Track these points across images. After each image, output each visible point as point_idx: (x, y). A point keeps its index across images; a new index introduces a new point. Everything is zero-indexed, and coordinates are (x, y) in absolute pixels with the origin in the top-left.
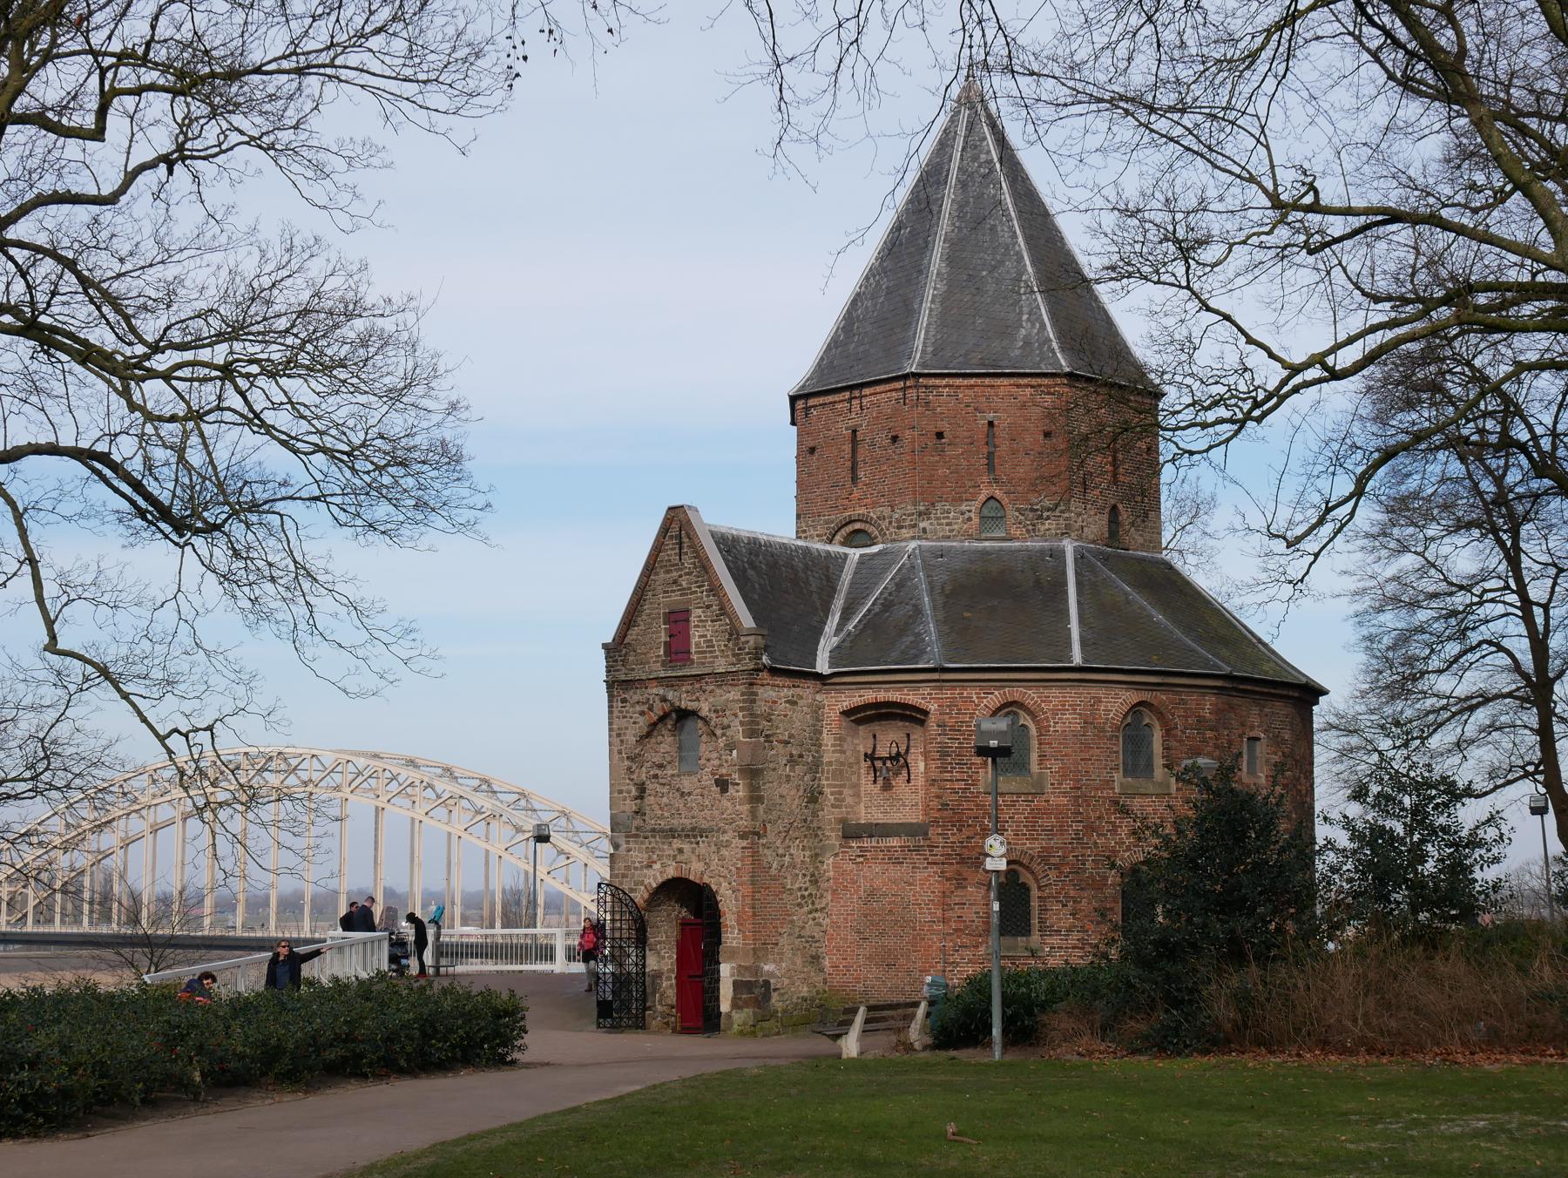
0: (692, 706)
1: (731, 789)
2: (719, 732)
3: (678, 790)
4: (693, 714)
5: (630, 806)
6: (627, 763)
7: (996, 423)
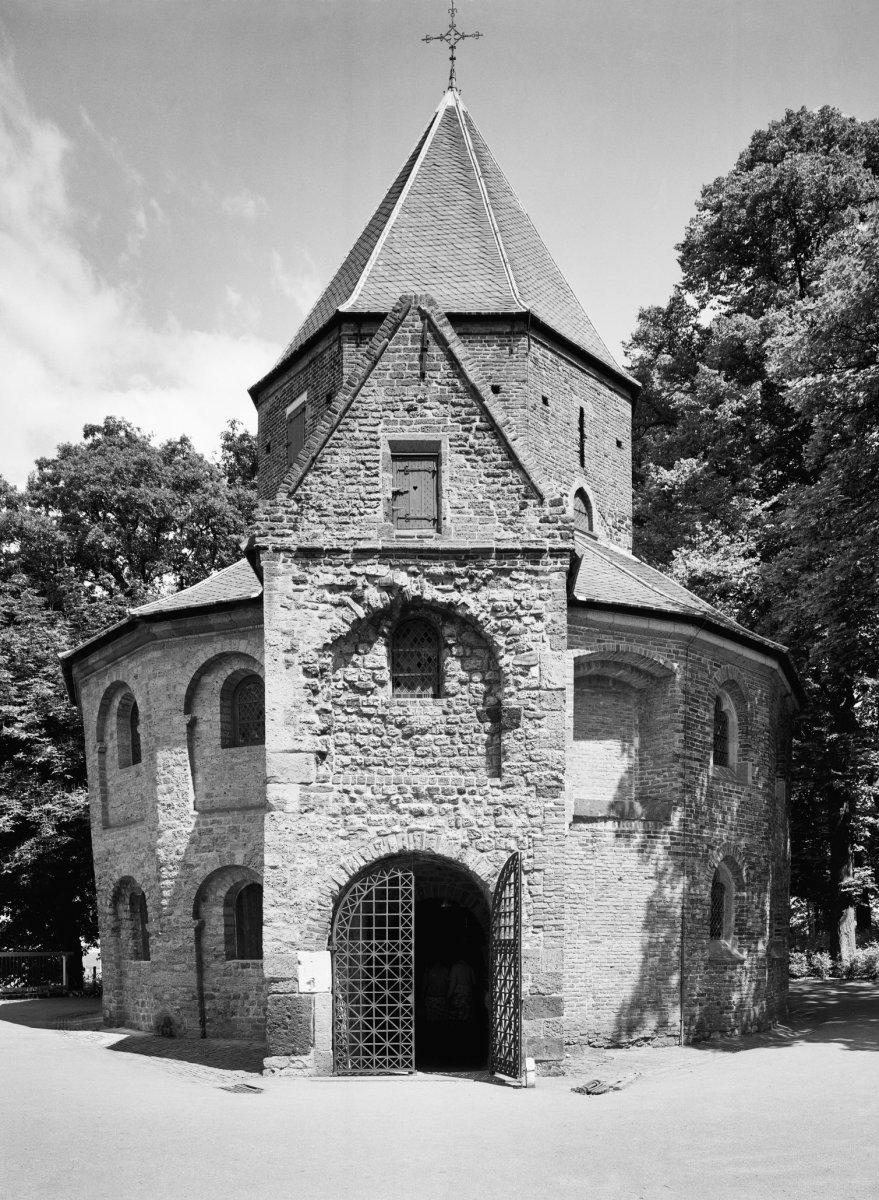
0: (442, 598)
1: (524, 721)
2: (501, 640)
3: (400, 726)
4: (448, 612)
5: (311, 742)
6: (305, 680)
7: (585, 411)
